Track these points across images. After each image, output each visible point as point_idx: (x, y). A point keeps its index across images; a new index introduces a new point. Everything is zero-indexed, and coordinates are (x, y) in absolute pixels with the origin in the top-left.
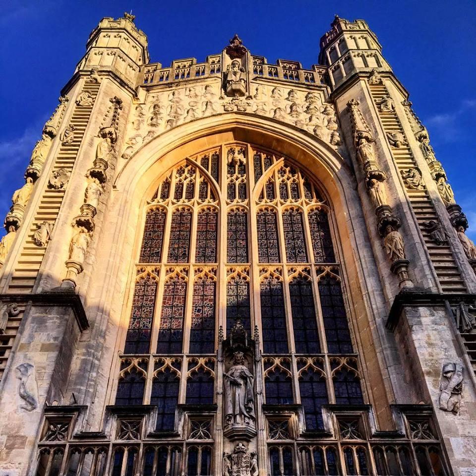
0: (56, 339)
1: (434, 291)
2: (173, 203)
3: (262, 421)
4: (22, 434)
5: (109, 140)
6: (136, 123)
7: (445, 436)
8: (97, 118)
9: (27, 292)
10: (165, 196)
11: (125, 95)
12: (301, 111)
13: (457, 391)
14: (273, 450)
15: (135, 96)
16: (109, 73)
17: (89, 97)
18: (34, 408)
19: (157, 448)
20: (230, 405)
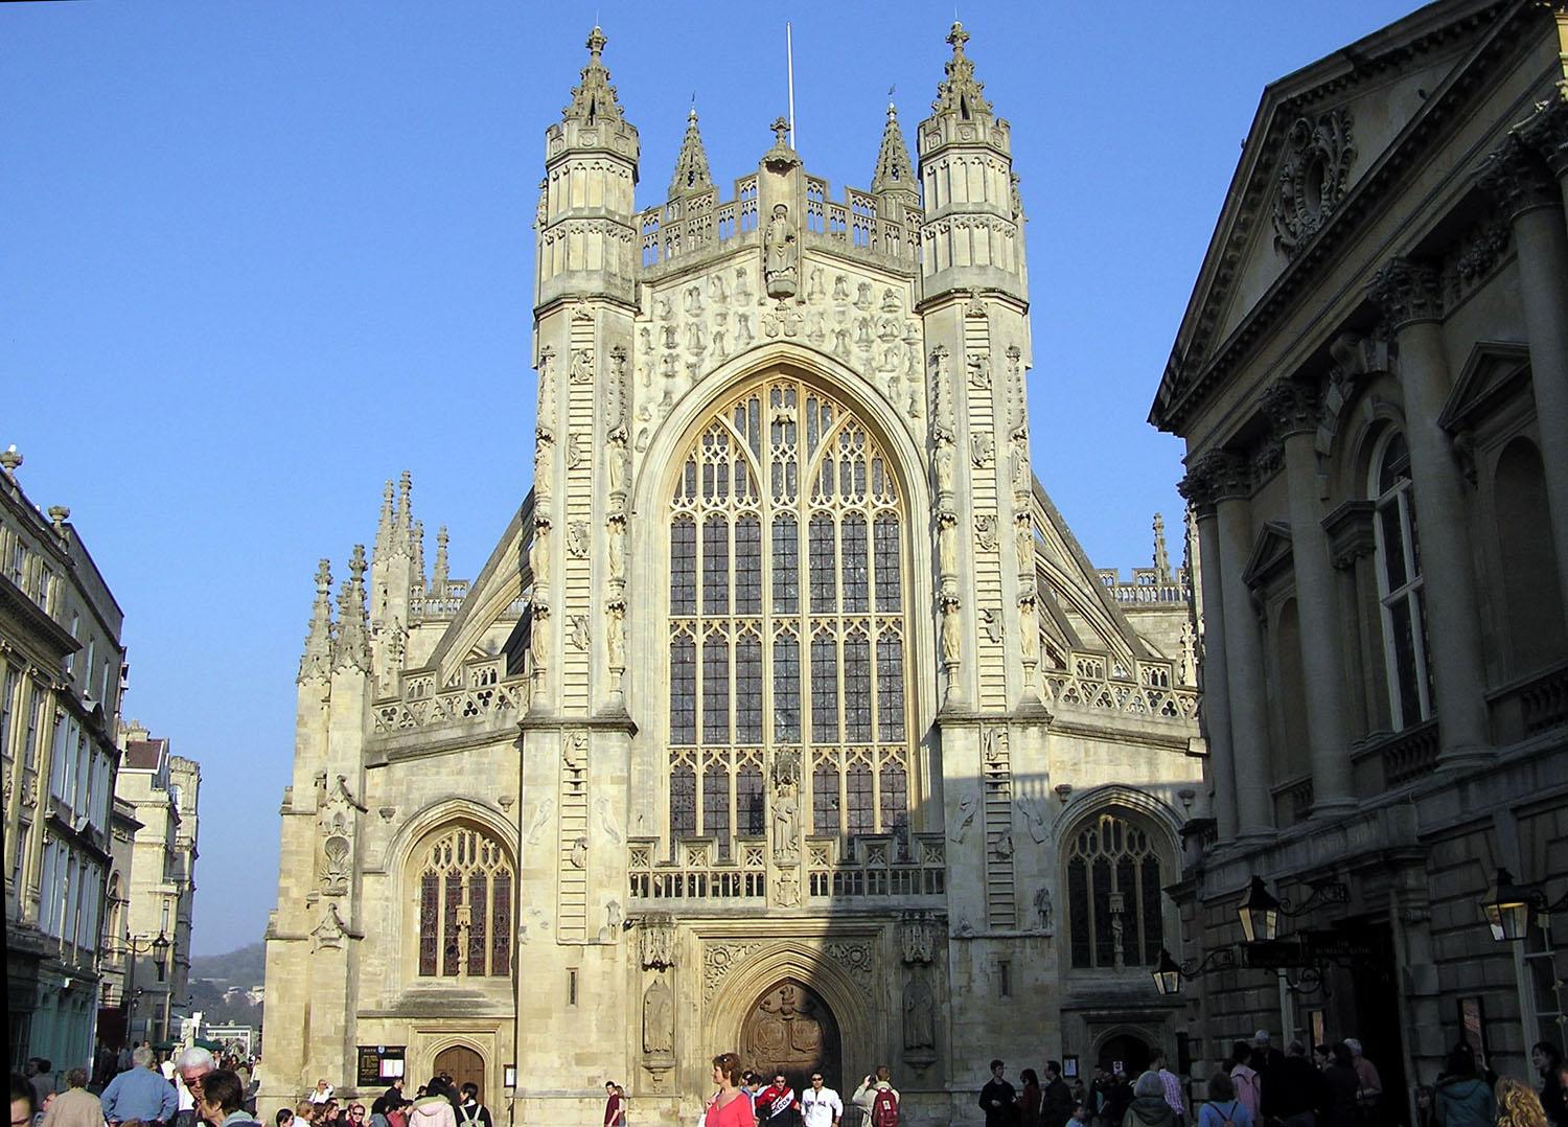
0: (621, 770)
1: (974, 709)
2: (704, 509)
3: (806, 849)
4: (615, 865)
5: (620, 442)
6: (645, 372)
7: (948, 864)
8: (602, 405)
9: (582, 714)
10: (691, 493)
11: (626, 315)
12: (873, 337)
13: (968, 822)
14: (813, 878)
15: (639, 312)
16: (600, 296)
17: (585, 362)
18: (619, 842)
19: (721, 875)
20: (778, 841)
